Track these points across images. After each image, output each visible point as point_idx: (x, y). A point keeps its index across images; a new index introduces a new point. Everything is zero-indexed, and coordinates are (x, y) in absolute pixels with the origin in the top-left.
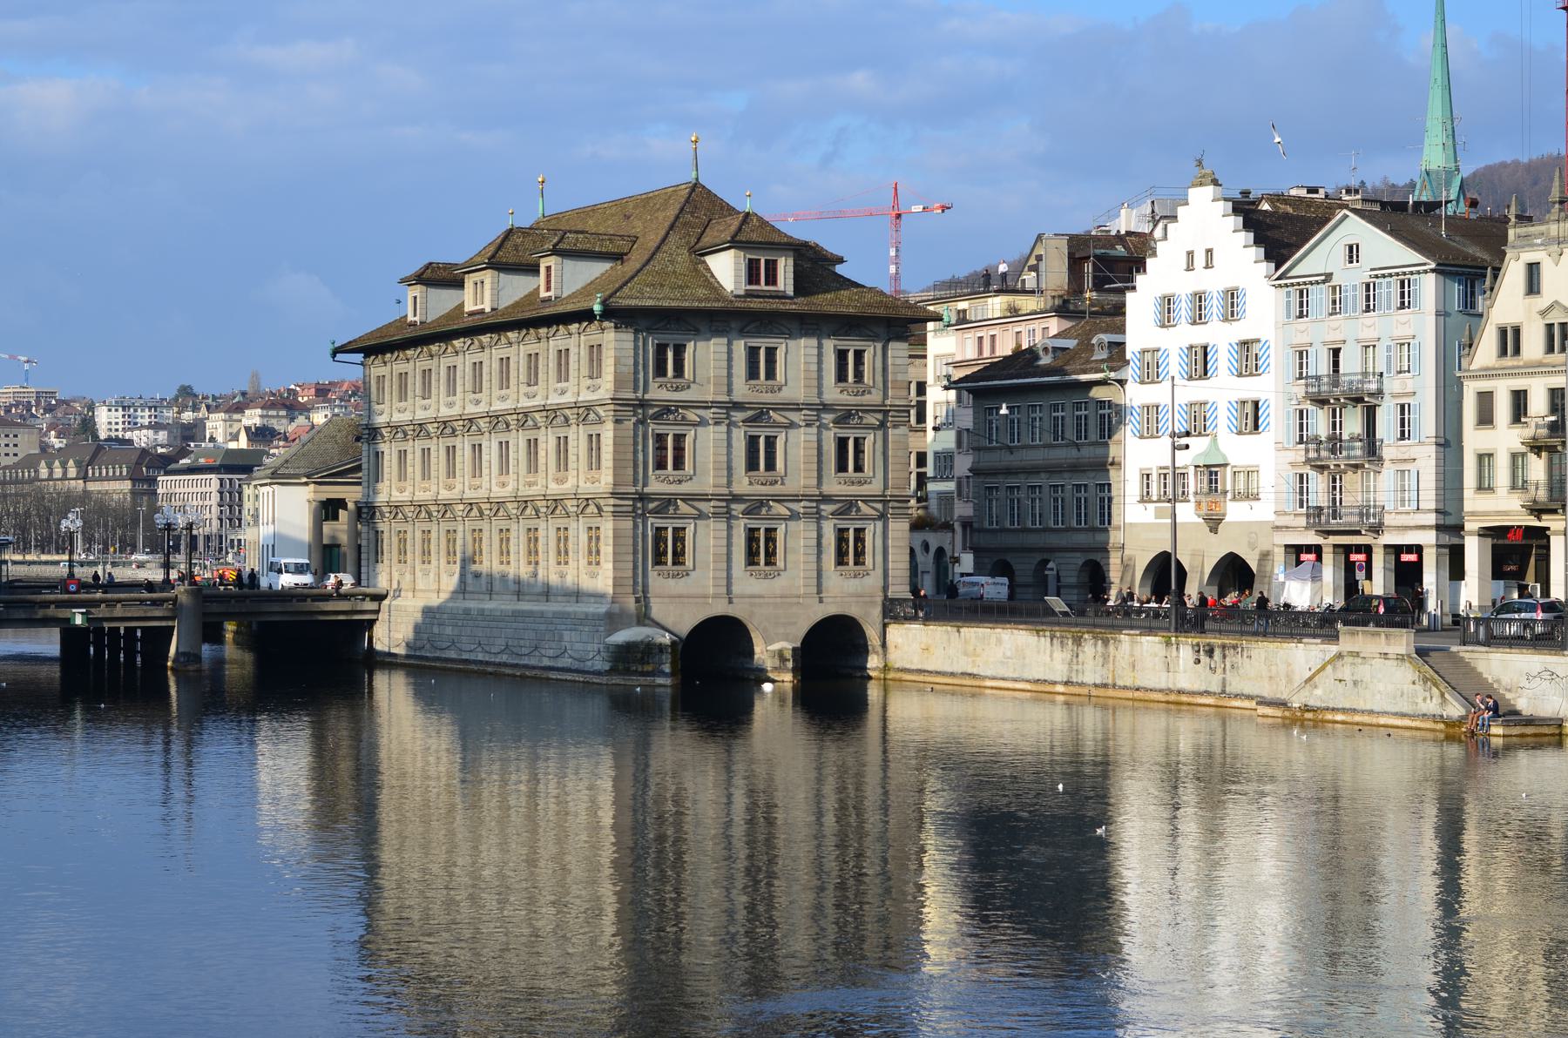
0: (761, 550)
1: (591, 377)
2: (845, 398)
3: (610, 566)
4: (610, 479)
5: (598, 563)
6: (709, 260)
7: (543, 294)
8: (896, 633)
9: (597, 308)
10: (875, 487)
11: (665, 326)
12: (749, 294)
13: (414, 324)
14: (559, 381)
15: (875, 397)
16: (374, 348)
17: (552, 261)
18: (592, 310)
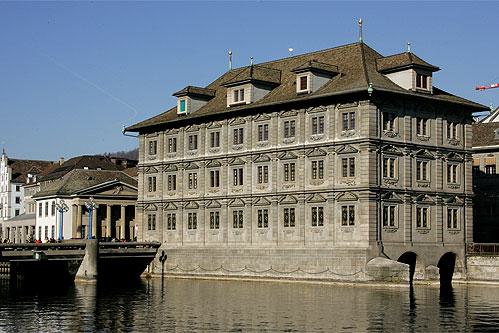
0: (422, 222)
1: (345, 128)
2: (450, 146)
3: (368, 225)
4: (366, 180)
5: (353, 224)
6: (390, 77)
7: (299, 90)
8: (476, 261)
9: (370, 90)
10: (459, 191)
11: (390, 103)
12: (417, 92)
13: (184, 115)
14: (315, 132)
15: (460, 147)
16: (144, 130)
17: (309, 75)
18: (366, 91)
